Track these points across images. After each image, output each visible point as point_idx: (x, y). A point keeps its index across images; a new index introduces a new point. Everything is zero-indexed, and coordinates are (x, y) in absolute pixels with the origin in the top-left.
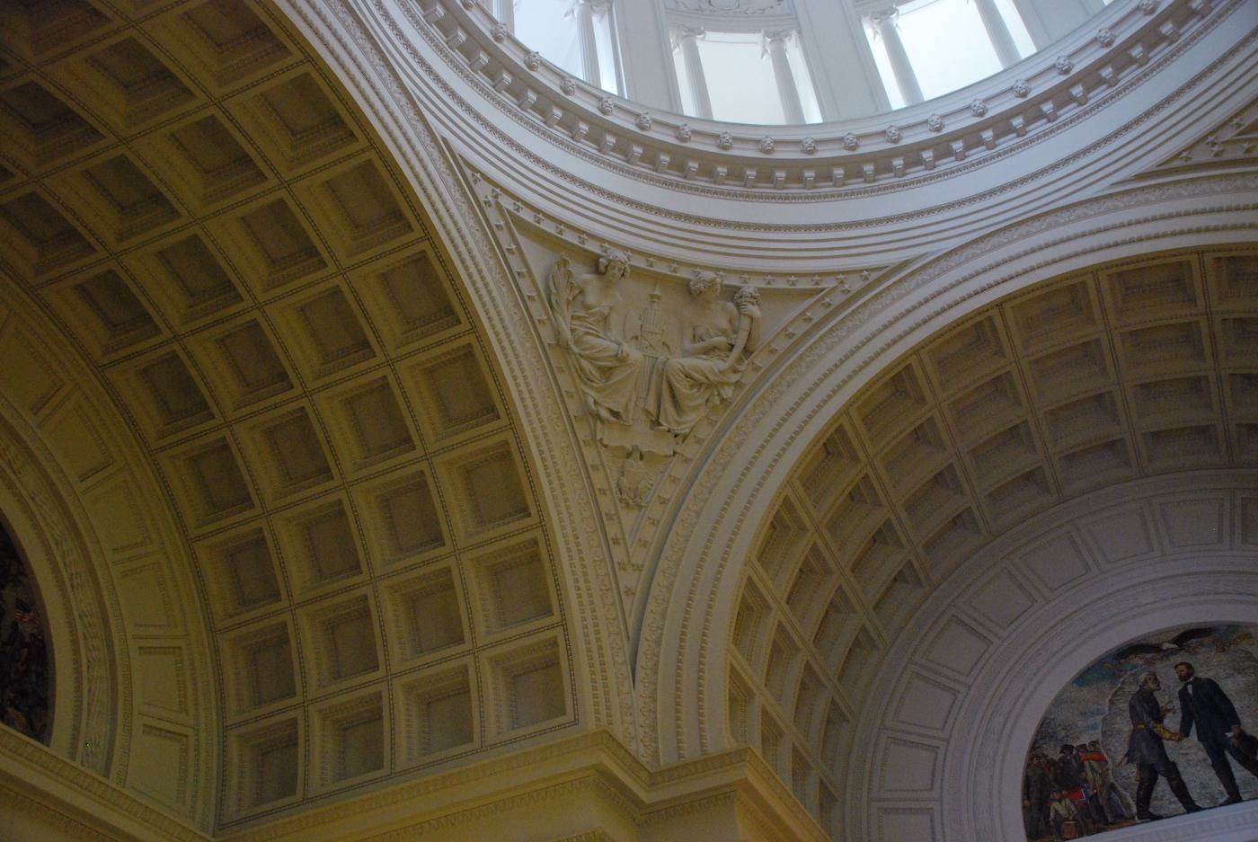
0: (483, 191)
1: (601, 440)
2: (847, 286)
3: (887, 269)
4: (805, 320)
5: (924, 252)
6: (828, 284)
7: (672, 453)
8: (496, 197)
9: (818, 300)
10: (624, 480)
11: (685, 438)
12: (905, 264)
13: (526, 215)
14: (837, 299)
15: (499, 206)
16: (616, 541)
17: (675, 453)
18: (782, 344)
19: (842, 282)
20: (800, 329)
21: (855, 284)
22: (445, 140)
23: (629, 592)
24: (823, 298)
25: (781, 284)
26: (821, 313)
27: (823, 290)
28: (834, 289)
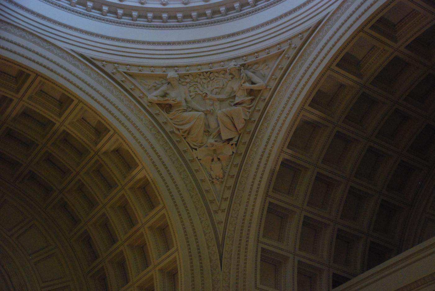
0: (109, 69)
1: (197, 158)
2: (293, 46)
3: (311, 30)
4: (279, 69)
5: (328, 12)
6: (285, 47)
7: (231, 153)
8: (116, 68)
9: (282, 58)
10: (212, 173)
11: (236, 145)
12: (319, 23)
13: (134, 71)
14: (292, 53)
15: (119, 71)
16: (212, 202)
17: (233, 152)
18: (273, 84)
19: (290, 45)
20: (279, 74)
21: (297, 42)
22: (82, 56)
23: (220, 223)
24: (284, 56)
25: (263, 56)
26: (285, 64)
27: (284, 51)
28: (289, 49)
